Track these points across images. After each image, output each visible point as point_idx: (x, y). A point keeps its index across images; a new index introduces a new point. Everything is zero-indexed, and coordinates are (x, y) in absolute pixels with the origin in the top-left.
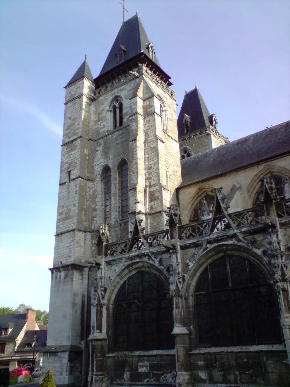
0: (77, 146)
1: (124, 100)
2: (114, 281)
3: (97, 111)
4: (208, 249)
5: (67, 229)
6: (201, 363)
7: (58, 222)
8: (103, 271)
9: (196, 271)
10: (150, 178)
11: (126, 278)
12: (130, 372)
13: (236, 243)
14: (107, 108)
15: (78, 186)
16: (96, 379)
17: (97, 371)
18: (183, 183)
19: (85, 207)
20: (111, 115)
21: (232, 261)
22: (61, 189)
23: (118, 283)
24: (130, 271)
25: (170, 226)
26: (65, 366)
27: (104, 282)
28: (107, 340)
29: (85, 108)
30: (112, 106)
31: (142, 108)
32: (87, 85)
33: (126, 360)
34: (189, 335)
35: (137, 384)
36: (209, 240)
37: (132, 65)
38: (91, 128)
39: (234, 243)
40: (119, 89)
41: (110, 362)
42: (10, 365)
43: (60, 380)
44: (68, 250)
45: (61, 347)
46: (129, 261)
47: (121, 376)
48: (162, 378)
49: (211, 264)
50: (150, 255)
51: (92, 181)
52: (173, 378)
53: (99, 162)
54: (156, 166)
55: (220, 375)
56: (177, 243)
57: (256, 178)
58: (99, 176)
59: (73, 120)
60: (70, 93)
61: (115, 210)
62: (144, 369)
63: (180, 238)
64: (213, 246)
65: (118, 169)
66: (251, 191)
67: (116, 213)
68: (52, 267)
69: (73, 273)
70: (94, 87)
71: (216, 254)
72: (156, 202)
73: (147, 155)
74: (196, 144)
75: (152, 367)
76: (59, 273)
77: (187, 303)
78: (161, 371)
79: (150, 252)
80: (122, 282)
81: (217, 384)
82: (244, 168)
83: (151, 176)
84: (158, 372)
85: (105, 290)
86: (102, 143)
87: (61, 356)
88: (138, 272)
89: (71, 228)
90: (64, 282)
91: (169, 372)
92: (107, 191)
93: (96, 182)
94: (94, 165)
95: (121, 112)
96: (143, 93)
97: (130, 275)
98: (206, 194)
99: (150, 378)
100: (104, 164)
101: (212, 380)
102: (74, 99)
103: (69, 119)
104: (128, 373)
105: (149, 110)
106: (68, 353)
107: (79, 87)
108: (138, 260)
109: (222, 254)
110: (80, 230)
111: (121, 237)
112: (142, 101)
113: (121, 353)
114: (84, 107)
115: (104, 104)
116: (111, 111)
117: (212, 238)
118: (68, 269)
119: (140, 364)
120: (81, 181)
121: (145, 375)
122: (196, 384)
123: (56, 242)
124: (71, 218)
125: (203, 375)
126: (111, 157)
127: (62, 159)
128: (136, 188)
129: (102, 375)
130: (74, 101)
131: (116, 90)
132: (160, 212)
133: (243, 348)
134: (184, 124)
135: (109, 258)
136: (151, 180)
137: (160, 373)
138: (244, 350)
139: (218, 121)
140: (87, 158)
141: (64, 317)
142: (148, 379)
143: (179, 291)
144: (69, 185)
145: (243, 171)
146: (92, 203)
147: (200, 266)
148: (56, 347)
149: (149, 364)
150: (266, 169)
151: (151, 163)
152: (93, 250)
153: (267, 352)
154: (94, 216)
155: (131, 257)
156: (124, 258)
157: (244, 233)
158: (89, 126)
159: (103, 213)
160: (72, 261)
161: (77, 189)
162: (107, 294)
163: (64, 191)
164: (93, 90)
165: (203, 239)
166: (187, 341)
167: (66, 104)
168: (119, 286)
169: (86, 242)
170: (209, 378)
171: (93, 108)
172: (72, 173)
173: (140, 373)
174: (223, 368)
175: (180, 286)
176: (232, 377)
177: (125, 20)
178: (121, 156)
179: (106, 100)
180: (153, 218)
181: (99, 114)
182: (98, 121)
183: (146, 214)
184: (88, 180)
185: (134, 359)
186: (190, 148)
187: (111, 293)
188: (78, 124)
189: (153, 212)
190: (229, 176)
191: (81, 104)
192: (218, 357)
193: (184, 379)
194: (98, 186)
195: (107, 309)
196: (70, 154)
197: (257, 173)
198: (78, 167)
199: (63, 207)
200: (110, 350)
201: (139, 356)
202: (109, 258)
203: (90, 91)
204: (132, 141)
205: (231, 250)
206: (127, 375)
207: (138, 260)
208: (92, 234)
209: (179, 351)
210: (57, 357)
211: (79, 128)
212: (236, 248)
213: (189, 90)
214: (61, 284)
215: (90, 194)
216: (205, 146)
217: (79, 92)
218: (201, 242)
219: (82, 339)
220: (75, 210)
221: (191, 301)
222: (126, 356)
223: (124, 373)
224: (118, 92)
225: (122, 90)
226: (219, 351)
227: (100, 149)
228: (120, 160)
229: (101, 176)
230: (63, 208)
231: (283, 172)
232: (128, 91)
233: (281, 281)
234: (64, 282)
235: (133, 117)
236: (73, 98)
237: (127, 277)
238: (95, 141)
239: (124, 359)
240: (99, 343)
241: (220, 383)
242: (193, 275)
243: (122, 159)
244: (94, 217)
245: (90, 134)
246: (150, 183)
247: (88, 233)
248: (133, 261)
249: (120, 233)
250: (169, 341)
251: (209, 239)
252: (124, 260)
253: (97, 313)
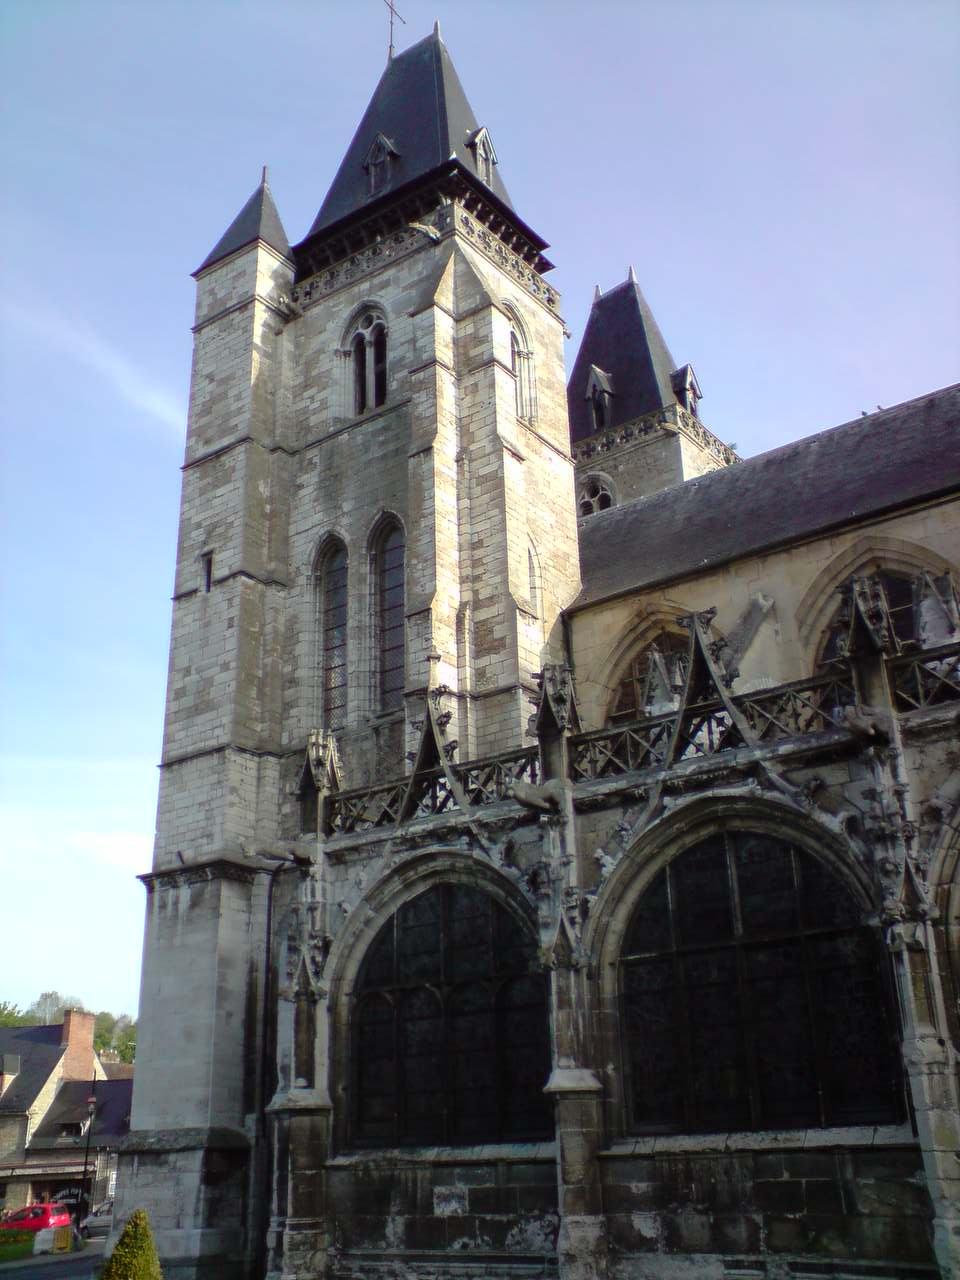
0: (233, 469)
1: (391, 316)
2: (355, 915)
3: (300, 355)
4: (666, 814)
5: (201, 745)
6: (639, 1187)
7: (168, 723)
8: (318, 886)
9: (626, 885)
10: (476, 578)
11: (393, 909)
12: (406, 1216)
13: (759, 791)
14: (336, 345)
15: (237, 601)
16: (292, 1238)
17: (296, 1214)
18: (584, 593)
19: (260, 673)
20: (350, 365)
21: (744, 854)
22: (180, 614)
23: (368, 922)
24: (408, 886)
25: (542, 737)
26: (193, 1197)
27: (323, 921)
28: (332, 1112)
29: (262, 342)
30: (350, 338)
31: (451, 345)
32: (267, 269)
33: (393, 1175)
34: (603, 1094)
35: (429, 1256)
36: (669, 783)
37: (418, 203)
38: (279, 409)
39: (752, 792)
40: (376, 281)
41: (339, 1185)
42: (9, 1195)
43: (175, 1243)
44: (201, 816)
45: (177, 1134)
46: (407, 850)
47: (376, 1231)
48: (512, 1236)
49: (675, 863)
50: (475, 830)
51: (283, 585)
52: (546, 1235)
53: (308, 524)
54: (497, 538)
55: (703, 1225)
56: (564, 793)
57: (826, 579)
58: (307, 571)
59: (224, 381)
60: (212, 292)
61: (361, 682)
62: (454, 1205)
63: (575, 776)
65: (369, 548)
66: (809, 621)
67: (364, 693)
68: (148, 869)
69: (219, 890)
70: (291, 275)
71: (695, 827)
72: (494, 658)
73: (466, 503)
74: (631, 466)
75: (478, 1201)
76: (172, 892)
77: (596, 990)
78: (507, 1212)
79: (474, 821)
80: (381, 921)
81: (692, 1255)
82: (788, 545)
83: (480, 571)
84: (497, 1217)
85: (325, 948)
86: (316, 460)
87: (178, 1164)
88: (434, 888)
89: (213, 743)
90: (189, 921)
91: (534, 1217)
92: (334, 619)
93: (296, 591)
94: (291, 534)
95: (380, 357)
96: (455, 294)
97: (407, 897)
98: (660, 632)
99: (473, 1237)
101: (675, 1243)
102: (227, 312)
103: (207, 381)
104: (400, 1220)
105: (473, 353)
106: (200, 1155)
107: (242, 274)
108: (435, 848)
109: (711, 829)
110: (242, 750)
111: (378, 771)
112: (451, 321)
113: (378, 1155)
114: (257, 340)
115: (325, 330)
116: (347, 354)
117: (680, 777)
118: (200, 876)
119: (438, 1190)
120: (247, 587)
122: (623, 1253)
123: (161, 788)
124: (213, 709)
125: (645, 1225)
126: (347, 507)
127: (182, 514)
128: (429, 610)
129: (312, 1226)
130: (225, 320)
131: (365, 286)
132: (510, 690)
133: (780, 1137)
134: (589, 398)
135: (341, 842)
136: (478, 586)
137: (504, 1218)
138: (782, 1145)
139: (702, 389)
140: (268, 508)
141: (189, 1035)
142: (466, 1240)
143: (571, 950)
144: (205, 600)
145: (784, 556)
146: (281, 658)
147: (642, 867)
148: (161, 1135)
149: (469, 1190)
150: (860, 550)
151: (478, 528)
152: (285, 816)
153: (855, 1150)
154: (288, 704)
155: (413, 839)
156: (390, 843)
157: (785, 760)
158: (273, 404)
159: (318, 692)
160: (215, 852)
161: (235, 612)
162: (332, 962)
163: (188, 620)
164: (287, 283)
165: (649, 781)
166: (595, 1113)
167: (197, 329)
168: (370, 934)
169: (261, 790)
170: (666, 1234)
171: (286, 343)
172: (216, 558)
173: (441, 1221)
174: (710, 1201)
175: (572, 933)
176: (740, 1232)
177: (398, 52)
178: (381, 503)
179: (332, 317)
180: (486, 709)
181: (309, 365)
182: (306, 386)
183: (461, 697)
184: (269, 582)
185: (420, 1174)
186: (610, 479)
187: (345, 958)
188: (238, 397)
189: (483, 688)
190: (736, 573)
191: (248, 330)
192: (696, 1166)
193: (583, 1240)
194: (303, 603)
195: (332, 1009)
196: (209, 495)
197: (828, 562)
198: (237, 541)
199: (187, 672)
200: (343, 1145)
201: (437, 1165)
202: (341, 842)
203: (278, 286)
204: (418, 453)
205: (738, 815)
206: (395, 1227)
208: (283, 761)
209: (568, 1147)
210: (165, 1170)
211: (240, 411)
212: (757, 808)
213: (608, 285)
214: (179, 927)
215: (275, 631)
216: (660, 473)
217: (241, 290)
218: (643, 788)
219: (248, 1108)
220: (225, 682)
221: (609, 984)
222: (392, 1162)
223: (386, 1221)
224: (371, 291)
225: (384, 285)
226: (698, 1148)
227: (310, 479)
228: (377, 518)
229: (315, 568)
230: (185, 676)
231: (915, 561)
232: (405, 289)
233: (905, 920)
234: (189, 921)
235: (421, 375)
236: (222, 309)
237: (399, 902)
238: (293, 453)
239: (389, 1173)
240: (306, 1120)
241: (701, 1251)
242: (618, 899)
243: (384, 512)
244: (288, 706)
245: (278, 432)
246: (476, 592)
247: (271, 759)
249: (376, 758)
250: (537, 1115)
251: (670, 779)
252: (388, 846)
253: (297, 1022)
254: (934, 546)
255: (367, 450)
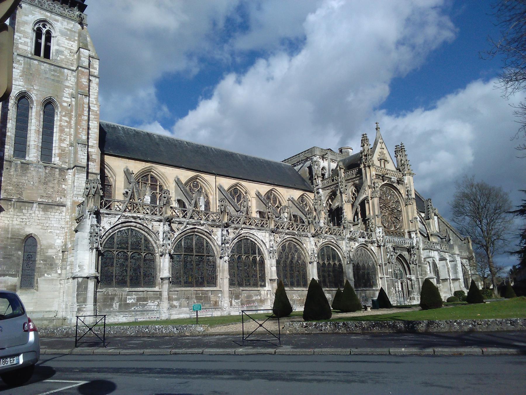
62: (132, 300)
64: (192, 227)
75: (139, 299)
100: (23, 90)
108: (133, 220)
111: (45, 180)
121: (133, 305)
125: (175, 303)
206: (116, 305)
207: (133, 220)
225: (57, 21)
248: (127, 220)
254: (166, 175)
255: (46, 73)
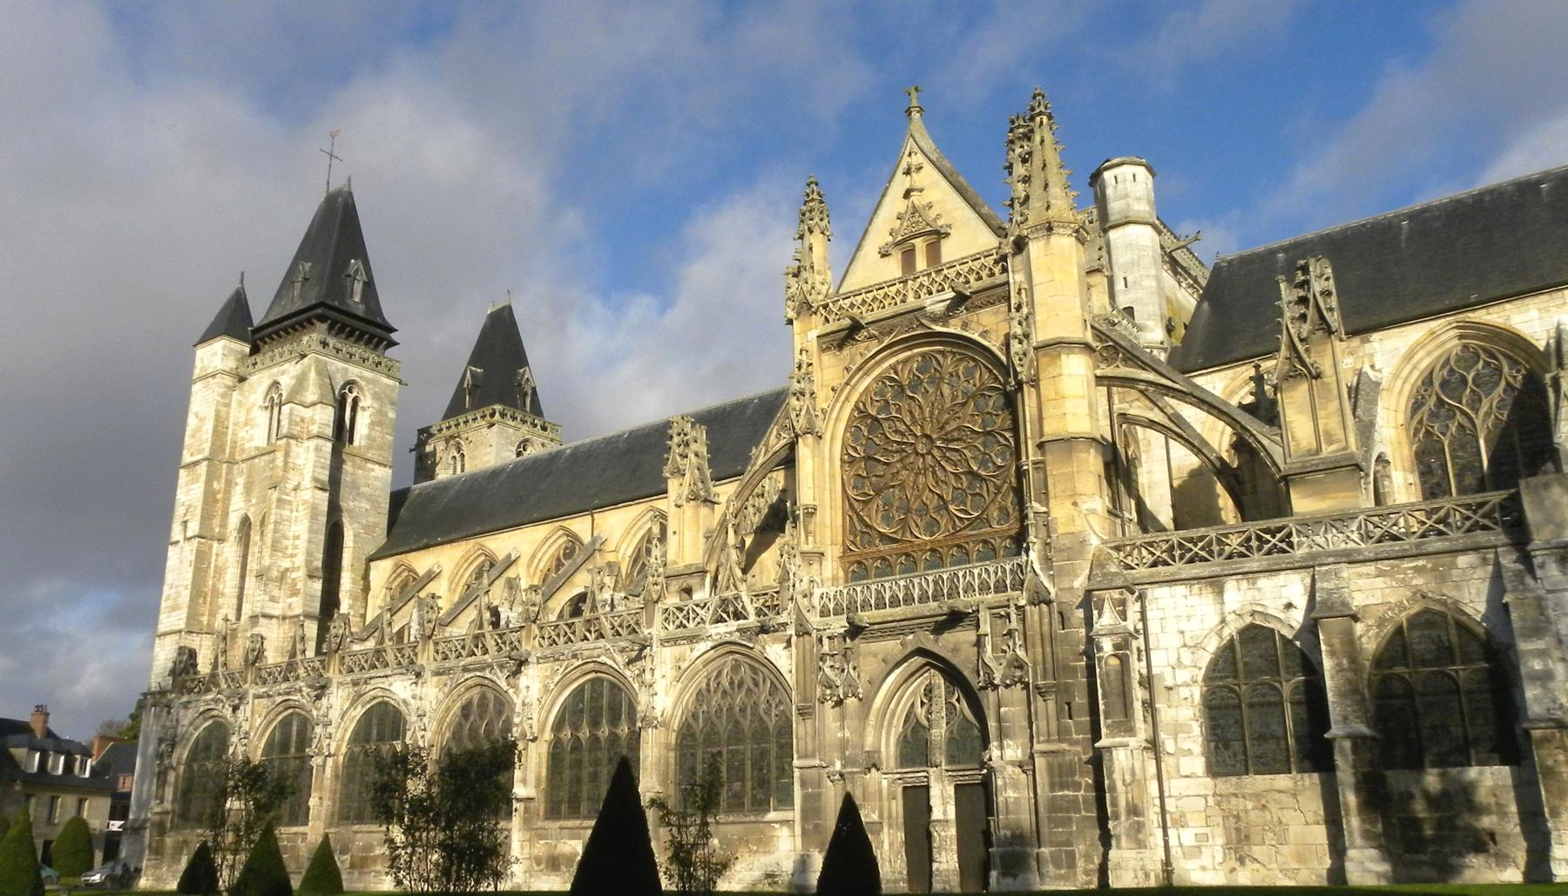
14: (261, 402)
20: (268, 413)
58: (235, 534)
126: (254, 501)
161: (193, 558)
198: (198, 518)
227: (241, 480)
